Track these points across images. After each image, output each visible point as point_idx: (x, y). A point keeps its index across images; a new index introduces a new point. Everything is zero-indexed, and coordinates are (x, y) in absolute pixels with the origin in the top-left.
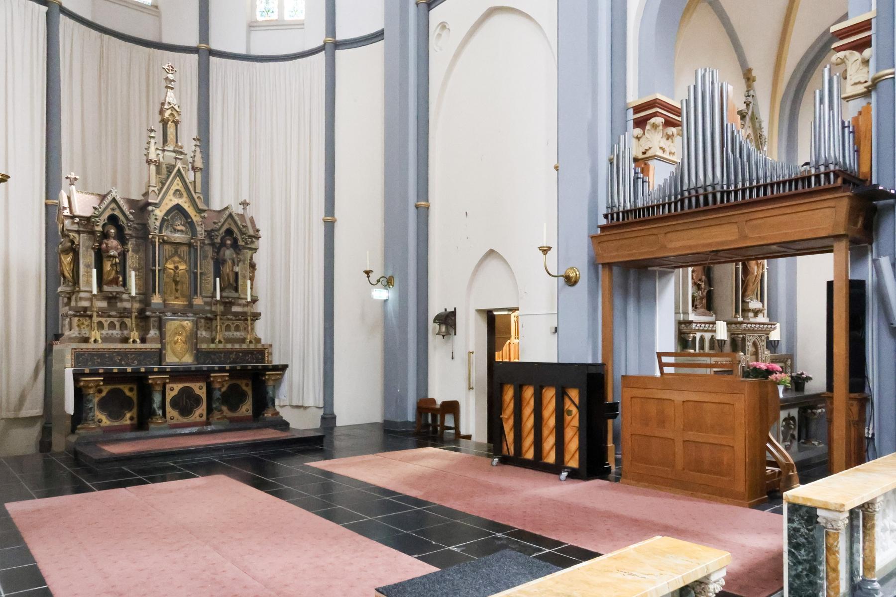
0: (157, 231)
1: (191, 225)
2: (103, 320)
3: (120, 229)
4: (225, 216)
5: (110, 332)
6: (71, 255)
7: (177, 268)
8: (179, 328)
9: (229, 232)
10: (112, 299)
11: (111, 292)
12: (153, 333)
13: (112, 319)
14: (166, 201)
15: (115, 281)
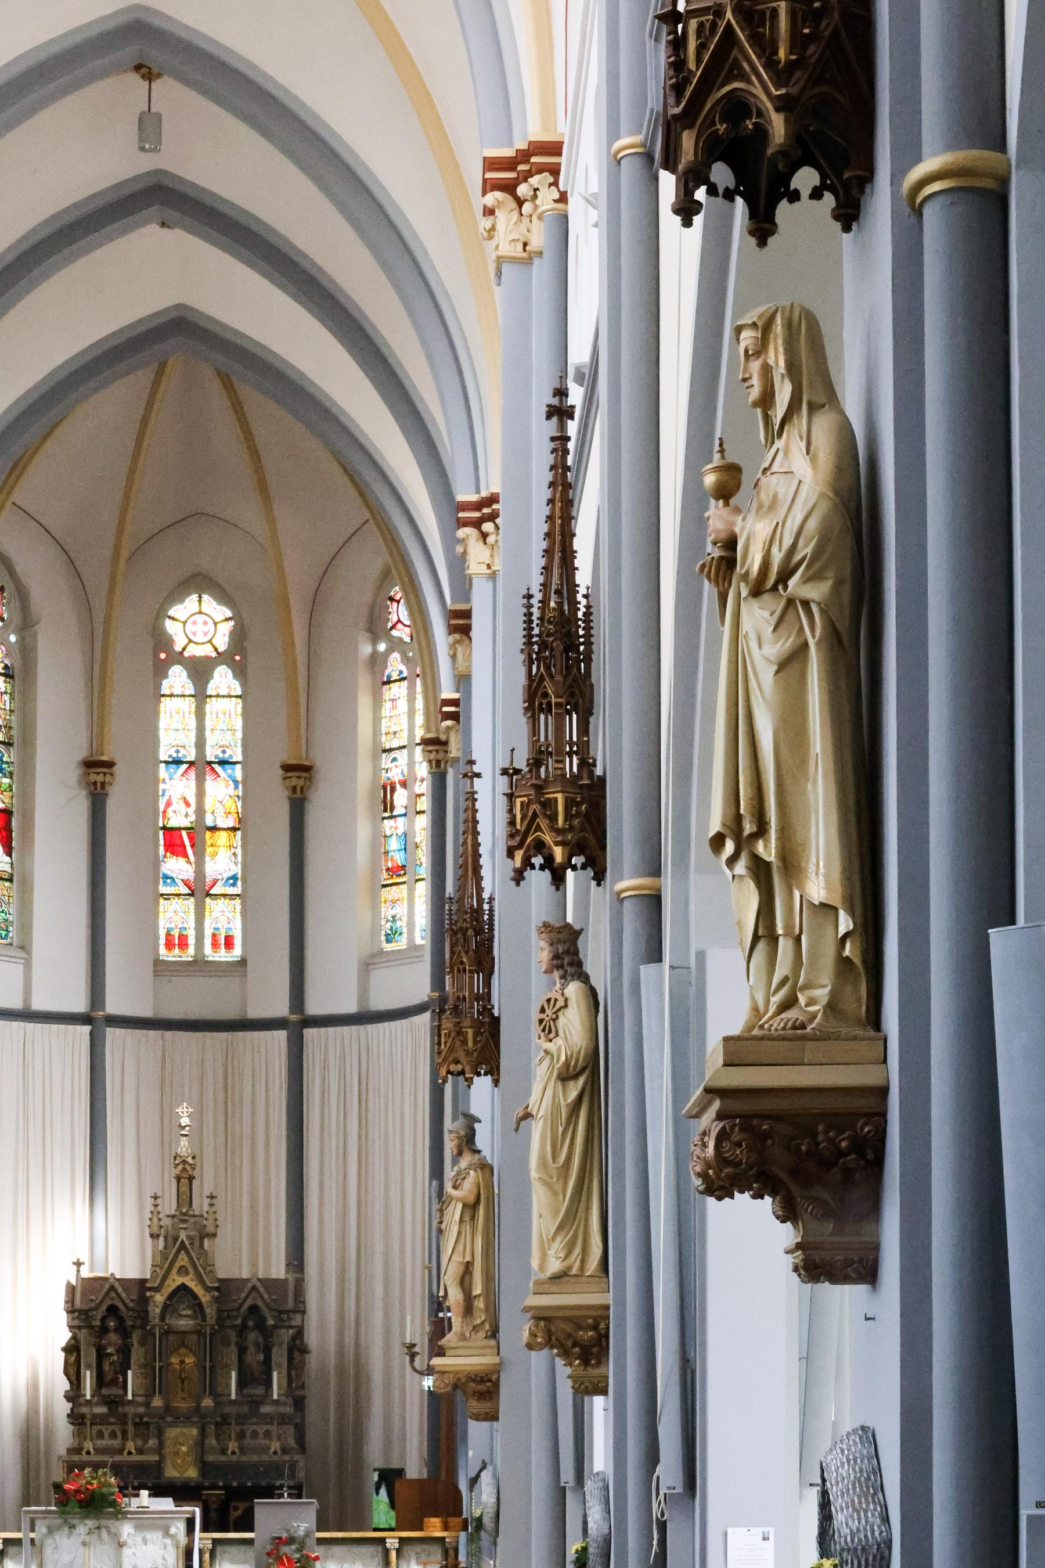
0: (157, 1321)
1: (198, 1307)
2: (103, 1428)
3: (121, 1320)
4: (247, 1290)
5: (110, 1442)
6: (75, 1355)
7: (182, 1362)
8: (181, 1438)
9: (254, 1309)
10: (114, 1403)
11: (109, 1396)
12: (152, 1442)
13: (113, 1427)
14: (168, 1282)
15: (114, 1382)
